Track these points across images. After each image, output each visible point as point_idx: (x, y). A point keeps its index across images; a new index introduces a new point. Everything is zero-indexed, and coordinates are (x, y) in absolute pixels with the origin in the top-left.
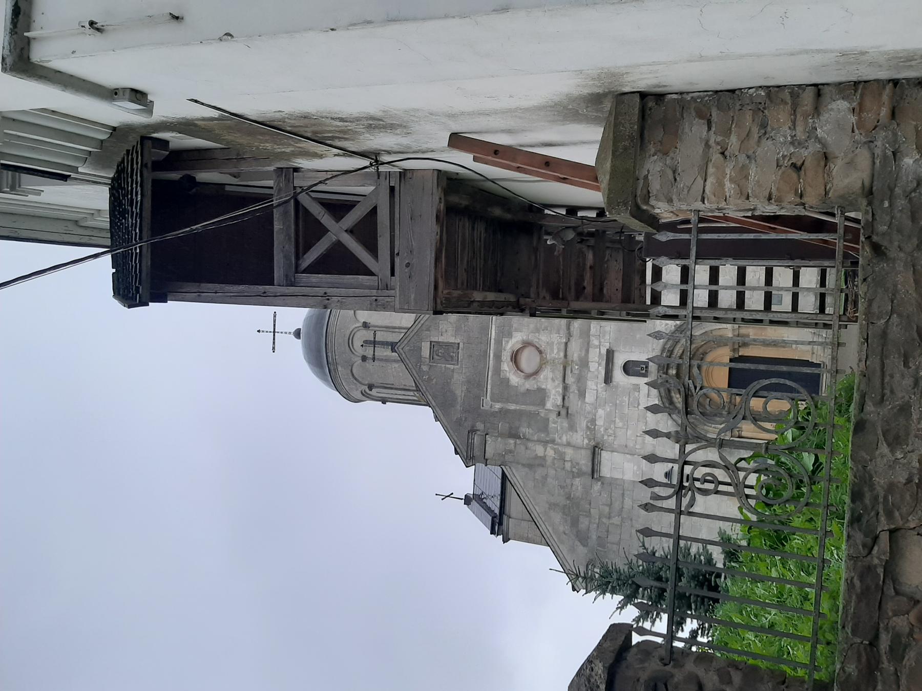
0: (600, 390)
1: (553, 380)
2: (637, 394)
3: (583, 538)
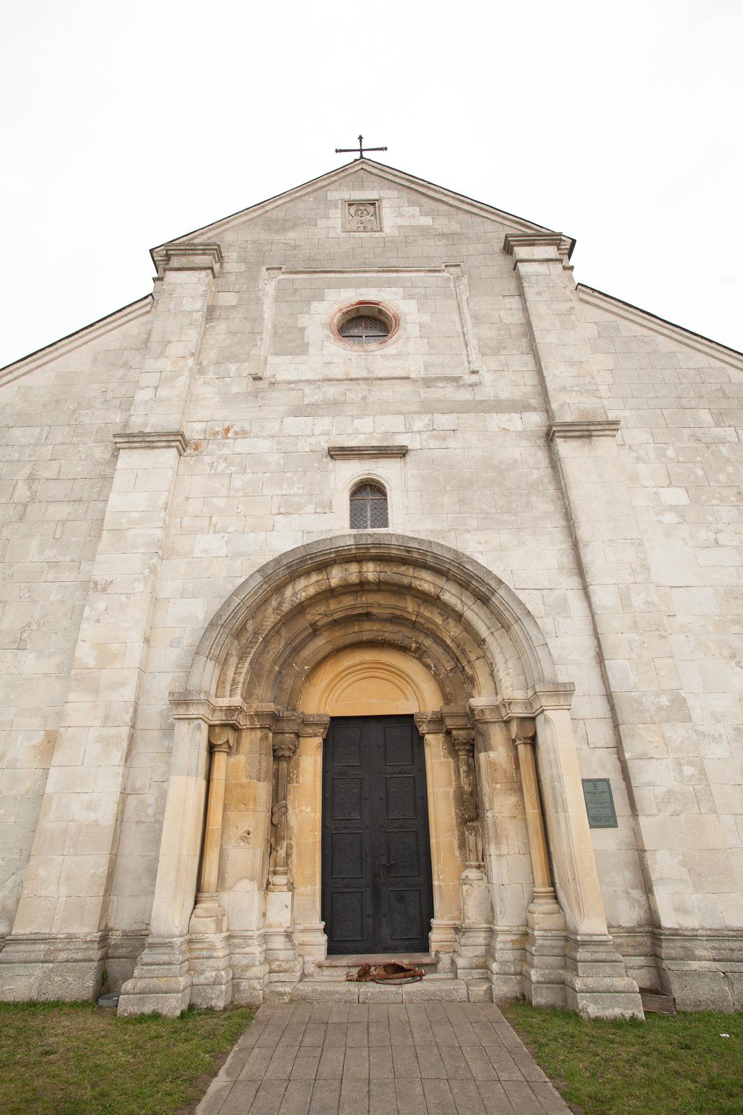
0: (313, 440)
2: (310, 508)
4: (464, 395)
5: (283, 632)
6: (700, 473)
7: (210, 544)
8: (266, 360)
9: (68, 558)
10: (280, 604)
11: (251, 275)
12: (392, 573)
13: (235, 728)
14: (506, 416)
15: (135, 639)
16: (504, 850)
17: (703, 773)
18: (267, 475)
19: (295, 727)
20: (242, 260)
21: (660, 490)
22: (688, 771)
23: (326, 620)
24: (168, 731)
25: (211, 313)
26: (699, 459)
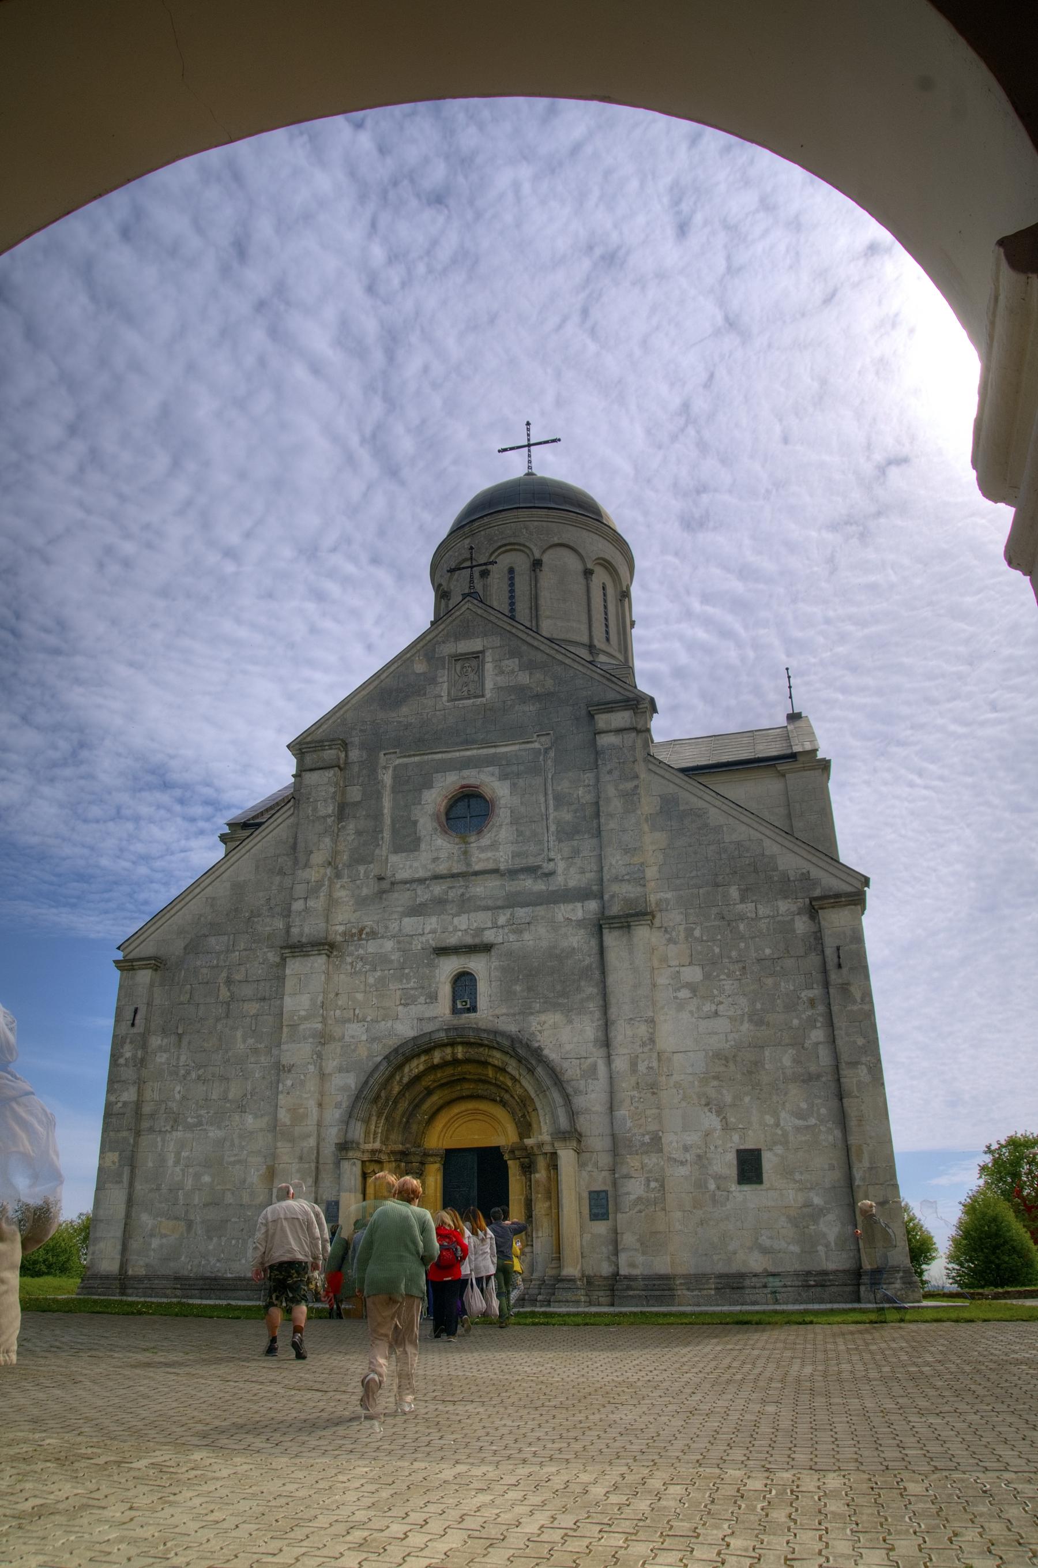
0: (423, 939)
1: (435, 860)
2: (422, 999)
3: (194, 947)
4: (540, 886)
5: (407, 1095)
6: (717, 950)
7: (355, 1031)
8: (387, 859)
9: (262, 1046)
10: (401, 1078)
11: (371, 767)
12: (473, 1052)
13: (379, 1162)
14: (571, 906)
15: (312, 1104)
16: (540, 1235)
17: (663, 1186)
18: (392, 972)
19: (419, 1159)
20: (363, 746)
21: (683, 969)
22: (653, 1185)
23: (436, 1084)
24: (337, 1164)
25: (343, 811)
26: (719, 937)
